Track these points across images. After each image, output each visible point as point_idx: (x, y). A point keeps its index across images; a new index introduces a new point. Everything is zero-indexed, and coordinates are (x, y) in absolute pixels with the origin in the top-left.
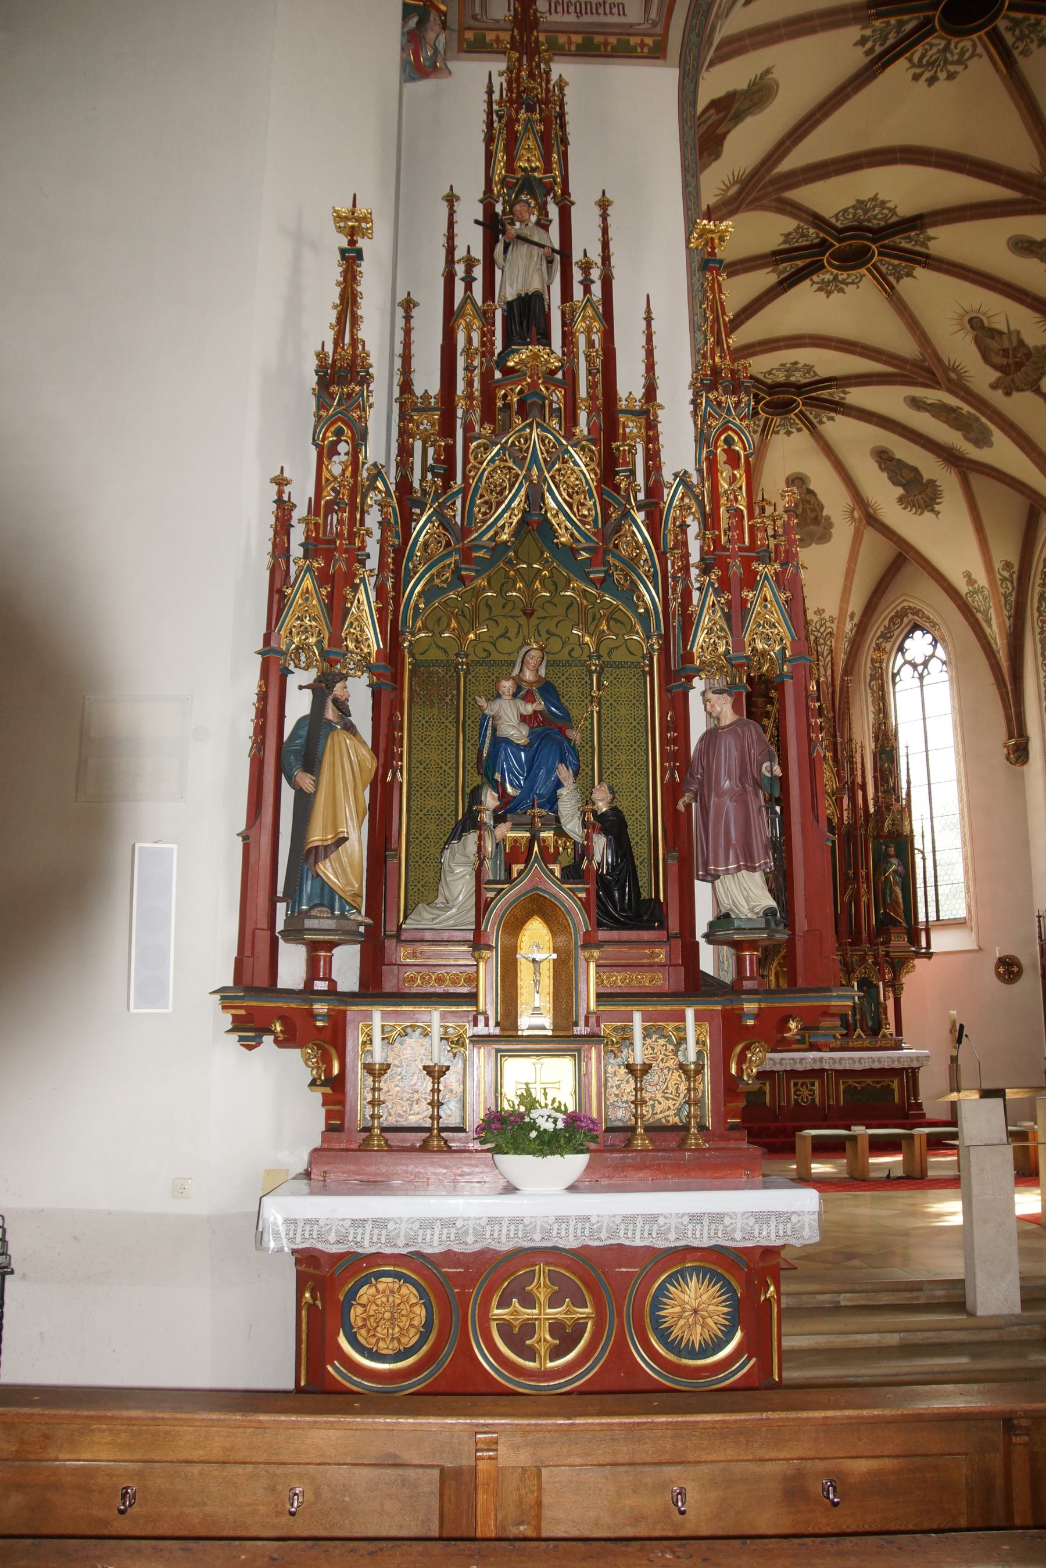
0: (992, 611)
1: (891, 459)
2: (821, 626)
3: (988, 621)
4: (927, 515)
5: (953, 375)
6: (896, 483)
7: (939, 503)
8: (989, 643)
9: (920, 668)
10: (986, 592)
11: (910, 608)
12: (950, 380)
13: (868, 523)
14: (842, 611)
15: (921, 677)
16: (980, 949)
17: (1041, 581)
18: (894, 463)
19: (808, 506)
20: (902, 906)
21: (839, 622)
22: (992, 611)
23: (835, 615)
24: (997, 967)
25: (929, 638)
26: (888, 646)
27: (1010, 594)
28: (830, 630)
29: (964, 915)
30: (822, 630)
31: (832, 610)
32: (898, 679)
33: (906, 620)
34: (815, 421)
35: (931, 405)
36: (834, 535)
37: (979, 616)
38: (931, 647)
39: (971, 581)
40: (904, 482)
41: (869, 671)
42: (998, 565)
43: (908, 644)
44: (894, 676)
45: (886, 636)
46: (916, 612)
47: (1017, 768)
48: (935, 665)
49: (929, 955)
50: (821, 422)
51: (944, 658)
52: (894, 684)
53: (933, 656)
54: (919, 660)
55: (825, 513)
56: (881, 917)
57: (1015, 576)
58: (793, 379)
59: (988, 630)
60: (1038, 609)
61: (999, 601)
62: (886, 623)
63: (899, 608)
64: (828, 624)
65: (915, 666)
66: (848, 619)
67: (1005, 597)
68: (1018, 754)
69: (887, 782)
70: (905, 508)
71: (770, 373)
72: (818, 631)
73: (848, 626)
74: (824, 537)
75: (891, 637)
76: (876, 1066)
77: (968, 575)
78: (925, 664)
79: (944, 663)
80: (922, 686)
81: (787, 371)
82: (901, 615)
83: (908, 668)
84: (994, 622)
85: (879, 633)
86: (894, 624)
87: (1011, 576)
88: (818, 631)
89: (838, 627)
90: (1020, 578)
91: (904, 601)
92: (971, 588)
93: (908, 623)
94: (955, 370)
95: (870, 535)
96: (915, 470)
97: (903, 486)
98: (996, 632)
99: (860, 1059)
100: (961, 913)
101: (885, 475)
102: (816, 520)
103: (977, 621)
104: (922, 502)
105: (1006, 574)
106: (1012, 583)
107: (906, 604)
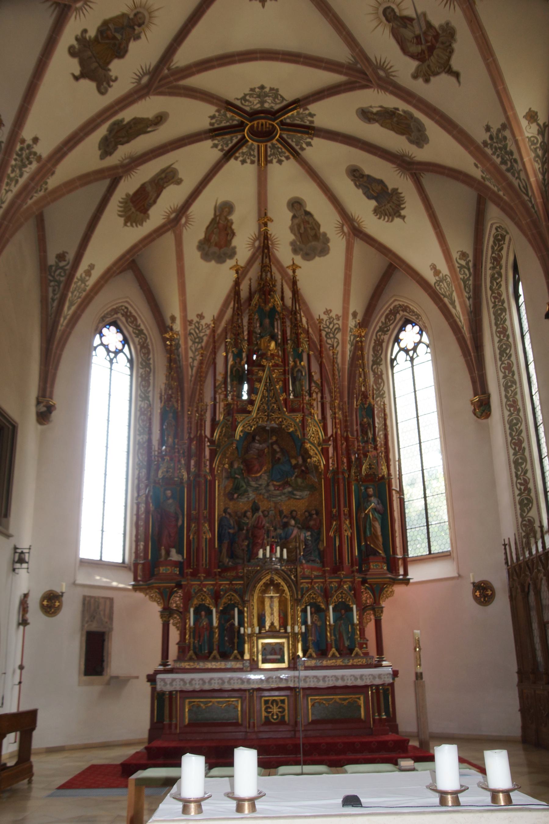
0: (454, 294)
1: (362, 176)
2: (330, 323)
3: (453, 303)
4: (397, 220)
5: (382, 73)
6: (369, 197)
7: (403, 209)
8: (455, 321)
9: (411, 353)
10: (449, 279)
11: (400, 306)
12: (380, 78)
13: (355, 235)
14: (345, 309)
15: (412, 359)
16: (460, 576)
17: (491, 265)
18: (365, 179)
19: (308, 226)
20: (380, 539)
21: (343, 319)
22: (454, 294)
23: (340, 313)
24: (474, 592)
25: (417, 329)
26: (386, 337)
27: (468, 279)
28: (337, 326)
29: (449, 549)
30: (331, 326)
31: (337, 310)
32: (395, 363)
33: (398, 317)
34: (297, 148)
35: (377, 113)
36: (331, 247)
37: (446, 300)
38: (419, 336)
39: (437, 272)
40: (375, 195)
41: (371, 358)
42: (455, 255)
43: (402, 335)
44: (392, 361)
45: (384, 330)
46: (405, 308)
48: (422, 348)
49: (406, 581)
50: (303, 149)
51: (428, 342)
52: (392, 367)
53: (420, 342)
55: (322, 230)
56: (363, 548)
57: (471, 264)
58: (266, 105)
59: (453, 311)
60: (491, 289)
61: (459, 284)
62: (383, 319)
63: (392, 307)
64: (335, 321)
65: (407, 351)
66: (351, 317)
67: (464, 282)
68: (482, 408)
69: (367, 434)
70: (380, 218)
71: (244, 98)
72: (328, 327)
73: (352, 323)
74: (324, 251)
75: (388, 331)
76: (340, 683)
77: (434, 267)
78: (415, 349)
79: (428, 346)
80: (413, 366)
81: (259, 96)
83: (402, 353)
84: (457, 304)
85: (378, 328)
86: (389, 320)
87: (467, 264)
88: (328, 327)
89: (343, 323)
90: (475, 265)
91: (395, 300)
92: (437, 278)
93: (400, 319)
94: (382, 67)
95: (359, 246)
96: (381, 182)
97: (376, 198)
99: (324, 677)
101: (360, 191)
102: (316, 237)
103: (445, 305)
104: (391, 210)
105: (463, 263)
106: (469, 269)
107: (396, 303)
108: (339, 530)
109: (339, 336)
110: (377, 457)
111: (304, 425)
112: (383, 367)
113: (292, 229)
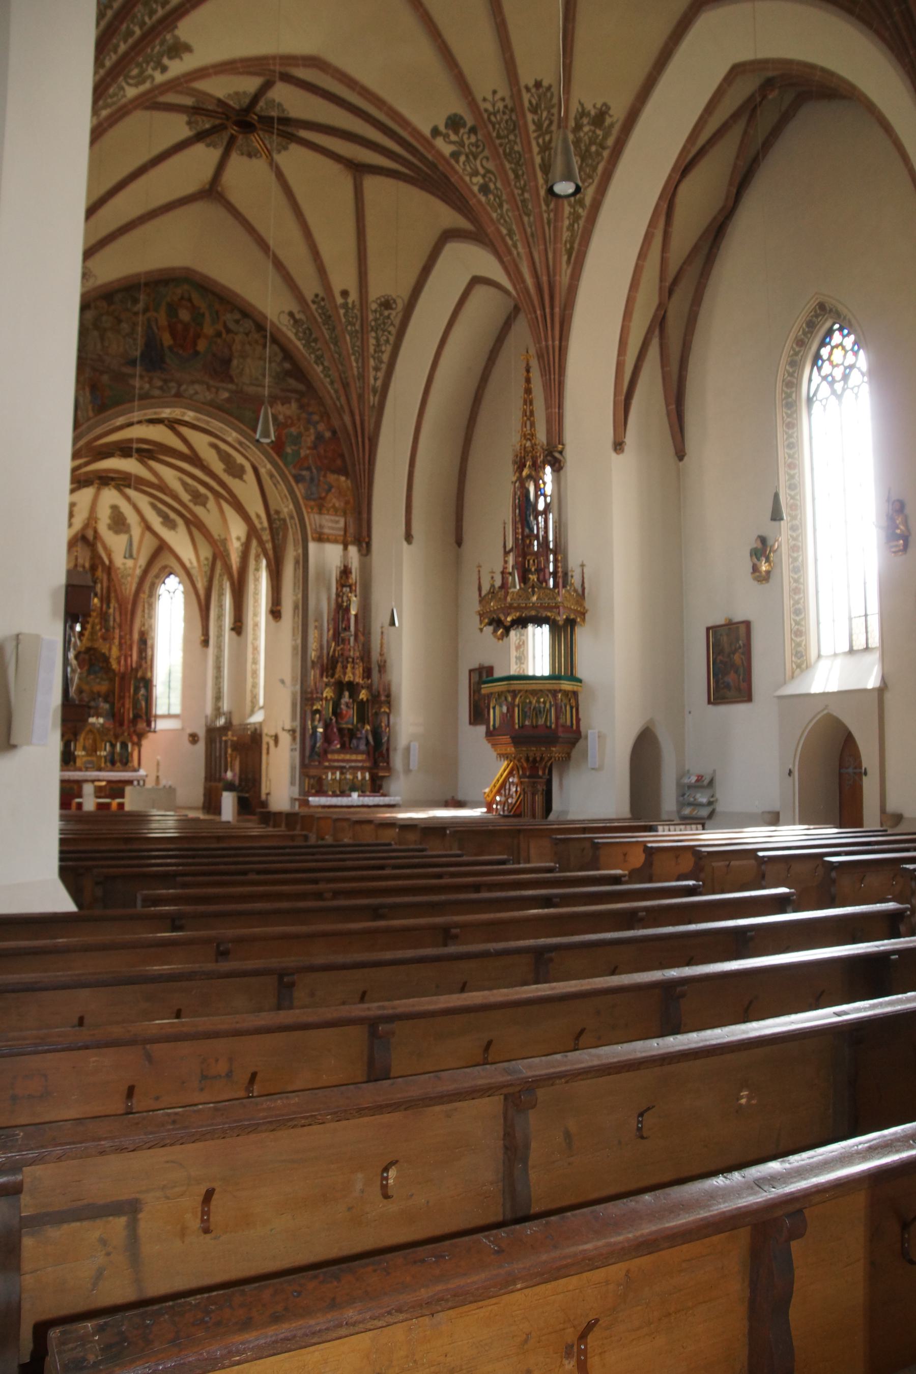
16: (183, 729)
25: (177, 579)
26: (157, 581)
39: (191, 563)
42: (202, 558)
43: (167, 581)
45: (157, 576)
46: (171, 568)
47: (204, 649)
49: (155, 732)
54: (172, 590)
73: (138, 572)
82: (165, 567)
95: (148, 535)
98: (201, 585)
100: (176, 709)
108: (123, 705)
109: (129, 579)
110: (146, 669)
111: (110, 649)
112: (153, 600)
113: (110, 518)
